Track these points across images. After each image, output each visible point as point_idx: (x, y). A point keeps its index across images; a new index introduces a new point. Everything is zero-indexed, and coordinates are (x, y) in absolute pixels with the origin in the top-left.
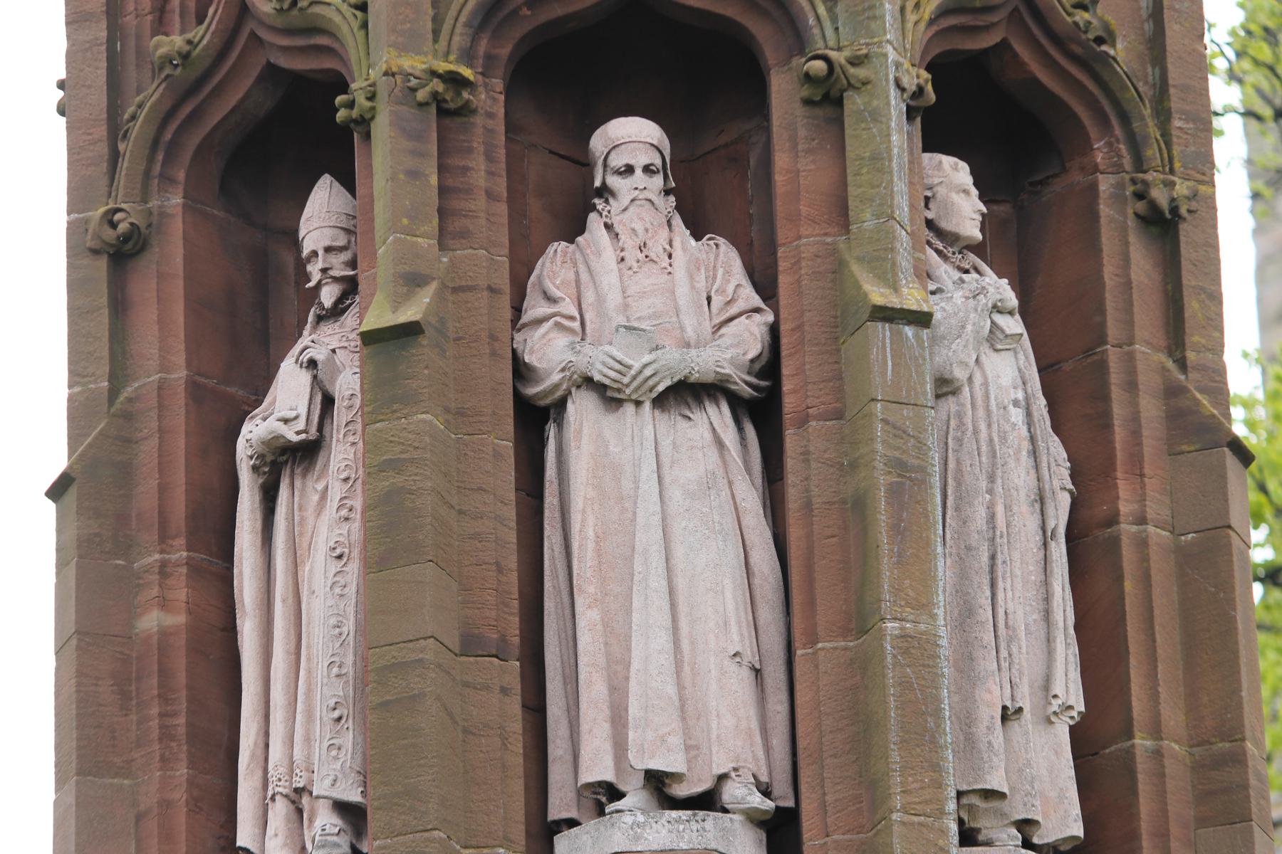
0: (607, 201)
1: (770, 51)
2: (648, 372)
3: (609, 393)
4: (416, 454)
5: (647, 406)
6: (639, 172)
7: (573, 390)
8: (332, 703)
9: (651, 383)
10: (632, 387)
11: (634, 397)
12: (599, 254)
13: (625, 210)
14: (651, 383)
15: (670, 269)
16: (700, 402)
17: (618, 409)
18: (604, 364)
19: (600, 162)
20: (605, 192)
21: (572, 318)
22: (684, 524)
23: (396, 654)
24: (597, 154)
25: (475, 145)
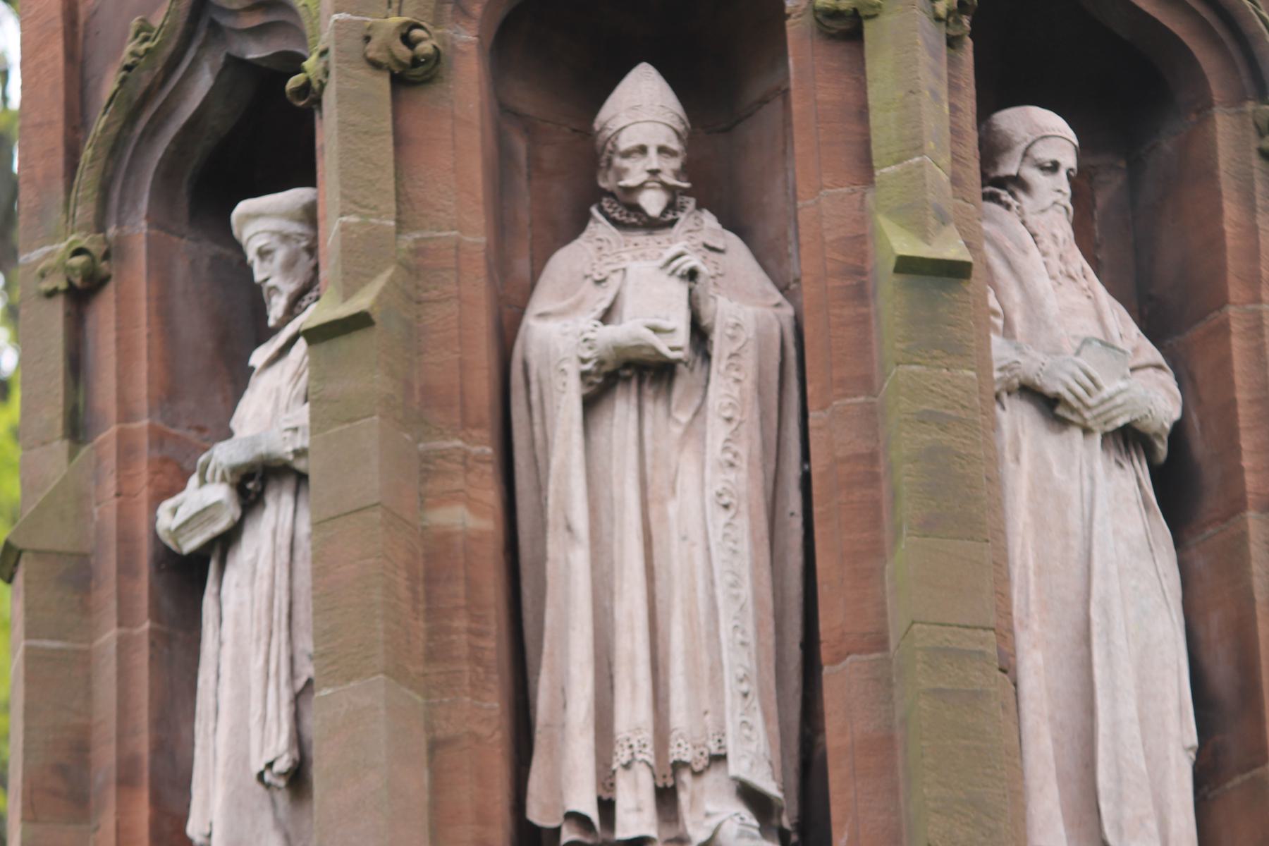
0: (1012, 194)
1: (1216, 88)
2: (1119, 400)
3: (1060, 411)
4: (962, 414)
5: (1098, 438)
6: (1062, 173)
7: (1004, 396)
8: (741, 672)
9: (1114, 413)
10: (1095, 412)
11: (1090, 424)
12: (1025, 252)
13: (1043, 211)
14: (1114, 413)
15: (1090, 293)
16: (1128, 451)
17: (1060, 431)
18: (1073, 376)
19: (1020, 149)
20: (1018, 183)
21: (995, 313)
22: (1133, 583)
23: (950, 638)
24: (1016, 139)
25: (963, 84)
